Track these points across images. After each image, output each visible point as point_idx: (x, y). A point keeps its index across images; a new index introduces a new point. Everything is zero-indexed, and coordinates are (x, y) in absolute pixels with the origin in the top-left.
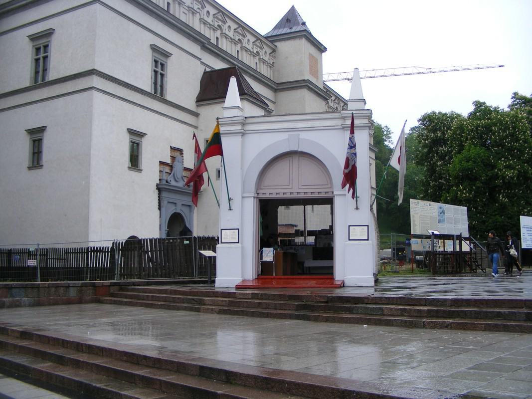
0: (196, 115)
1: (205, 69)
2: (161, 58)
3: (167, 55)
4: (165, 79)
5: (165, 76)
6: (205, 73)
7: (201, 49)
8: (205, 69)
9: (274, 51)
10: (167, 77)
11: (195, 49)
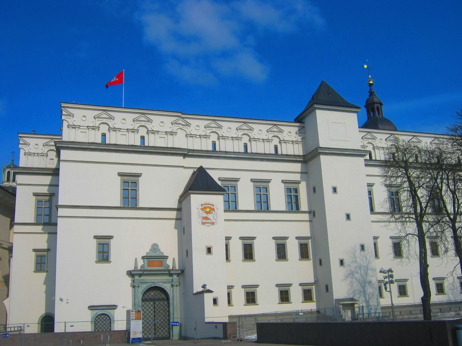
9: (303, 127)
10: (138, 191)
11: (178, 160)
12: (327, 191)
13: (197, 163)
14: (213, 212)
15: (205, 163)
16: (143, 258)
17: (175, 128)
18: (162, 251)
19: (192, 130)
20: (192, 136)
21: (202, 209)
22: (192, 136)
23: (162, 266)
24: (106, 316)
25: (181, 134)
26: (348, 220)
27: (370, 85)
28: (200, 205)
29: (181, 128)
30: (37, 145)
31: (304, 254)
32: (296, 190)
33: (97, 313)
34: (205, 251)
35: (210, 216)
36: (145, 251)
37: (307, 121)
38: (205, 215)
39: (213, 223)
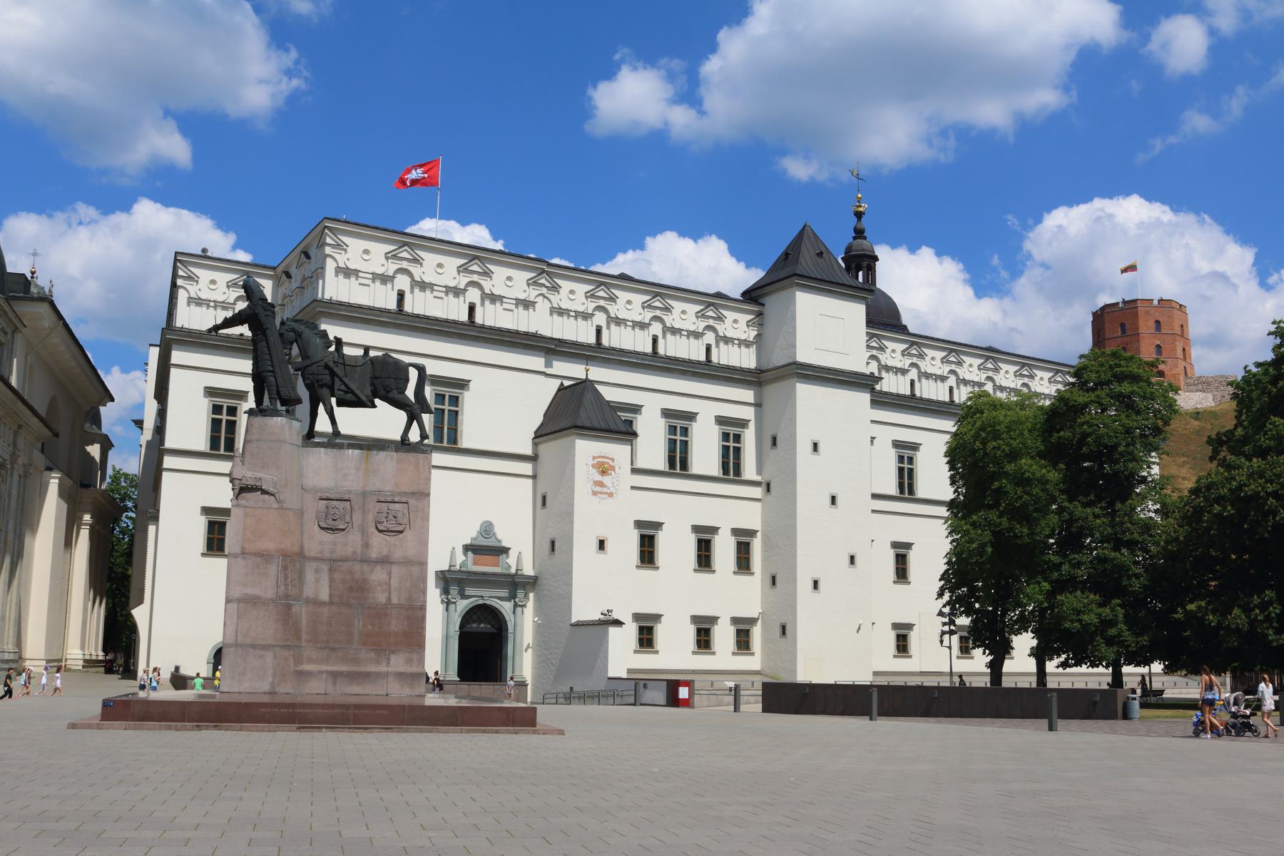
0: (533, 459)
1: (562, 384)
3: (462, 384)
4: (460, 417)
5: (460, 413)
6: (562, 389)
7: (546, 353)
8: (562, 384)
9: (760, 314)
10: (462, 415)
11: (537, 362)
13: (576, 370)
14: (613, 472)
15: (597, 373)
16: (467, 548)
17: (532, 294)
18: (499, 537)
19: (561, 299)
20: (561, 312)
21: (593, 466)
22: (561, 312)
23: (497, 565)
25: (543, 306)
26: (833, 506)
28: (591, 458)
29: (545, 297)
30: (213, 282)
31: (743, 562)
32: (737, 438)
34: (595, 545)
35: (606, 480)
36: (469, 534)
37: (773, 303)
38: (598, 477)
39: (611, 495)
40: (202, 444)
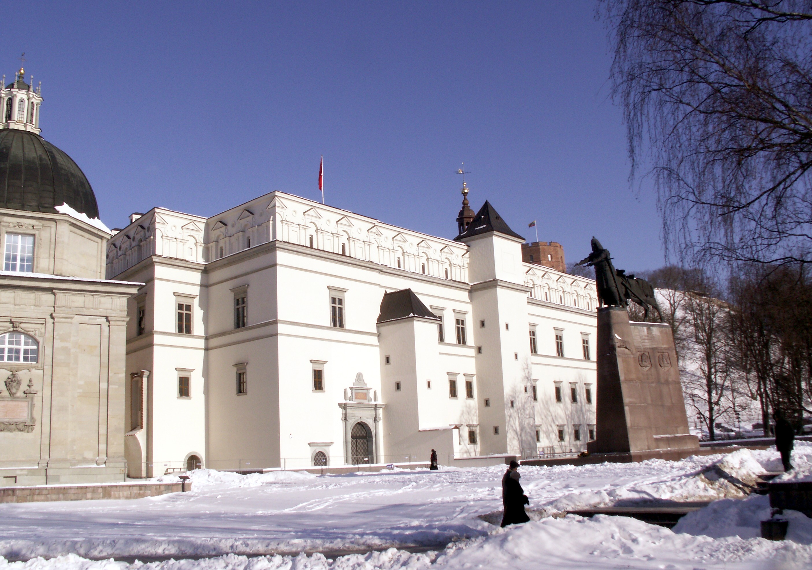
1: (386, 292)
2: (337, 295)
3: (343, 291)
4: (343, 311)
6: (386, 295)
8: (386, 292)
12: (502, 327)
23: (365, 399)
24: (322, 455)
27: (465, 194)
33: (315, 450)
40: (173, 327)
